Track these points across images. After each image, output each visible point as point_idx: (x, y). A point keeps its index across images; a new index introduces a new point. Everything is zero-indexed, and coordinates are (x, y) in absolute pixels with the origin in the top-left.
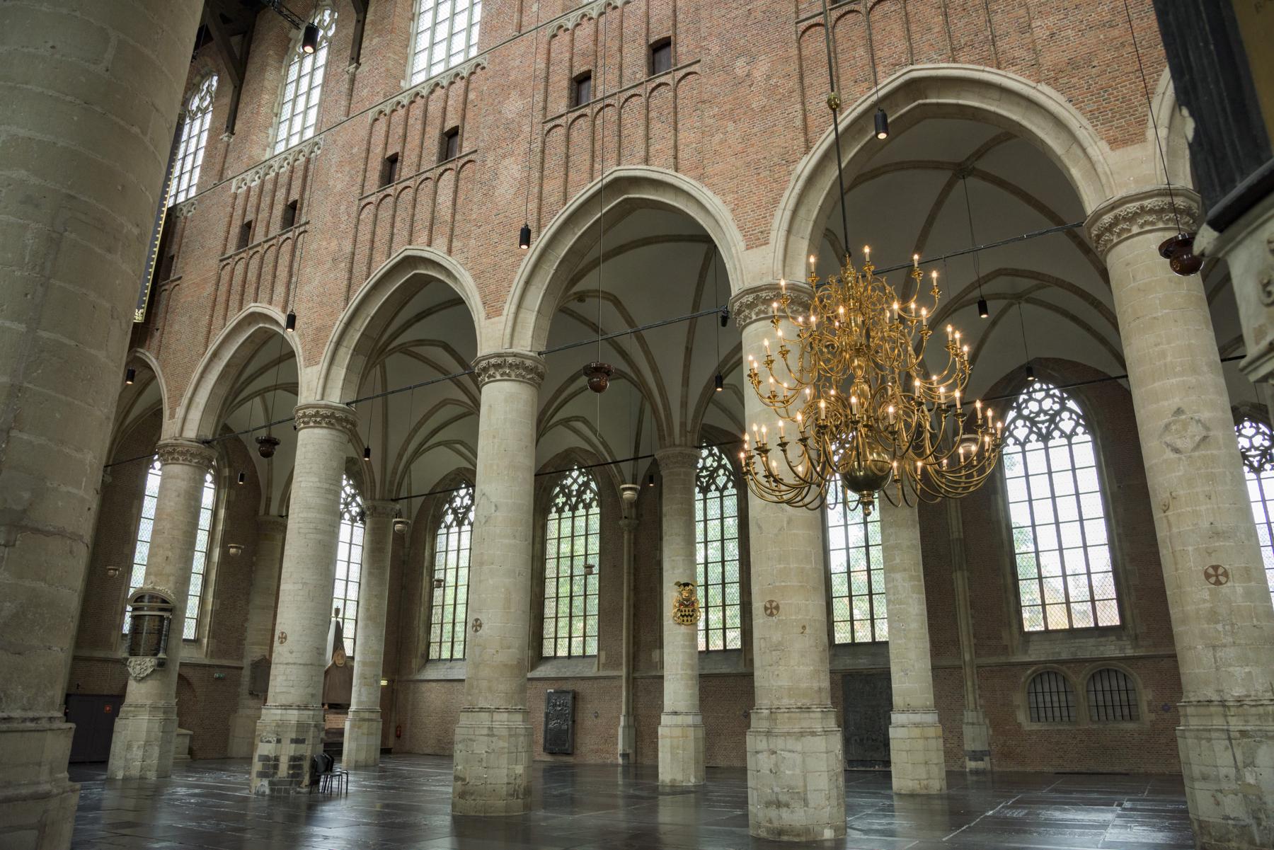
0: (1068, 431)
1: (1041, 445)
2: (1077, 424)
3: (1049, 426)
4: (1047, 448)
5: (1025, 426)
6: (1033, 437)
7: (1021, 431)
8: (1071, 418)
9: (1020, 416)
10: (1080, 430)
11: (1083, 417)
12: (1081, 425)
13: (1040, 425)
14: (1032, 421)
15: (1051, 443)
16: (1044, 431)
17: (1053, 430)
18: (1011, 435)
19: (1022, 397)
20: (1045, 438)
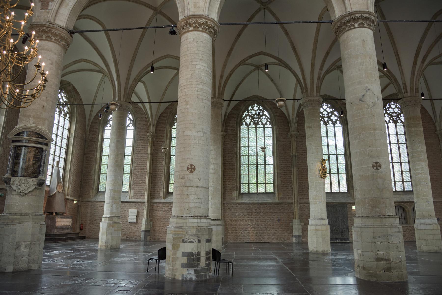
0: (248, 123)
1: (254, 126)
2: (268, 121)
3: (258, 120)
4: (256, 128)
5: (249, 119)
6: (252, 123)
7: (248, 121)
8: (265, 119)
9: (248, 115)
10: (268, 123)
11: (133, 121)
12: (132, 123)
13: (255, 119)
14: (252, 117)
15: (258, 126)
16: (256, 121)
17: (259, 122)
18: (244, 121)
19: (250, 108)
20: (256, 124)
